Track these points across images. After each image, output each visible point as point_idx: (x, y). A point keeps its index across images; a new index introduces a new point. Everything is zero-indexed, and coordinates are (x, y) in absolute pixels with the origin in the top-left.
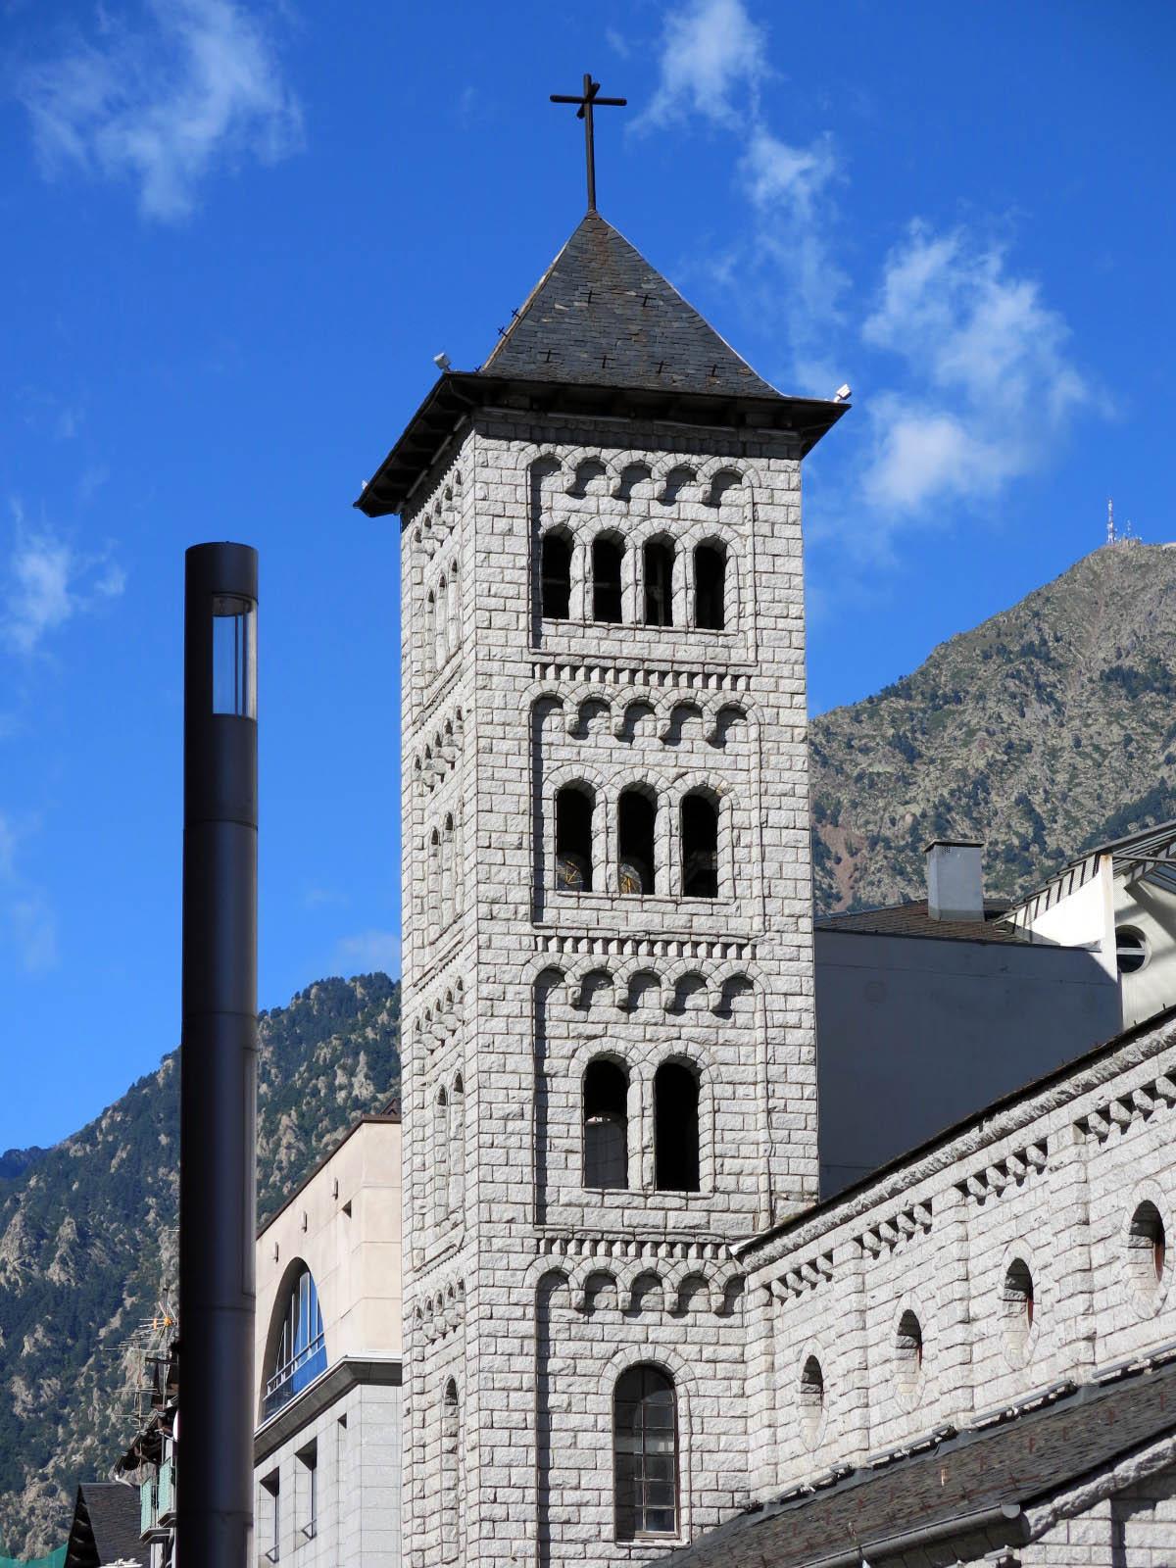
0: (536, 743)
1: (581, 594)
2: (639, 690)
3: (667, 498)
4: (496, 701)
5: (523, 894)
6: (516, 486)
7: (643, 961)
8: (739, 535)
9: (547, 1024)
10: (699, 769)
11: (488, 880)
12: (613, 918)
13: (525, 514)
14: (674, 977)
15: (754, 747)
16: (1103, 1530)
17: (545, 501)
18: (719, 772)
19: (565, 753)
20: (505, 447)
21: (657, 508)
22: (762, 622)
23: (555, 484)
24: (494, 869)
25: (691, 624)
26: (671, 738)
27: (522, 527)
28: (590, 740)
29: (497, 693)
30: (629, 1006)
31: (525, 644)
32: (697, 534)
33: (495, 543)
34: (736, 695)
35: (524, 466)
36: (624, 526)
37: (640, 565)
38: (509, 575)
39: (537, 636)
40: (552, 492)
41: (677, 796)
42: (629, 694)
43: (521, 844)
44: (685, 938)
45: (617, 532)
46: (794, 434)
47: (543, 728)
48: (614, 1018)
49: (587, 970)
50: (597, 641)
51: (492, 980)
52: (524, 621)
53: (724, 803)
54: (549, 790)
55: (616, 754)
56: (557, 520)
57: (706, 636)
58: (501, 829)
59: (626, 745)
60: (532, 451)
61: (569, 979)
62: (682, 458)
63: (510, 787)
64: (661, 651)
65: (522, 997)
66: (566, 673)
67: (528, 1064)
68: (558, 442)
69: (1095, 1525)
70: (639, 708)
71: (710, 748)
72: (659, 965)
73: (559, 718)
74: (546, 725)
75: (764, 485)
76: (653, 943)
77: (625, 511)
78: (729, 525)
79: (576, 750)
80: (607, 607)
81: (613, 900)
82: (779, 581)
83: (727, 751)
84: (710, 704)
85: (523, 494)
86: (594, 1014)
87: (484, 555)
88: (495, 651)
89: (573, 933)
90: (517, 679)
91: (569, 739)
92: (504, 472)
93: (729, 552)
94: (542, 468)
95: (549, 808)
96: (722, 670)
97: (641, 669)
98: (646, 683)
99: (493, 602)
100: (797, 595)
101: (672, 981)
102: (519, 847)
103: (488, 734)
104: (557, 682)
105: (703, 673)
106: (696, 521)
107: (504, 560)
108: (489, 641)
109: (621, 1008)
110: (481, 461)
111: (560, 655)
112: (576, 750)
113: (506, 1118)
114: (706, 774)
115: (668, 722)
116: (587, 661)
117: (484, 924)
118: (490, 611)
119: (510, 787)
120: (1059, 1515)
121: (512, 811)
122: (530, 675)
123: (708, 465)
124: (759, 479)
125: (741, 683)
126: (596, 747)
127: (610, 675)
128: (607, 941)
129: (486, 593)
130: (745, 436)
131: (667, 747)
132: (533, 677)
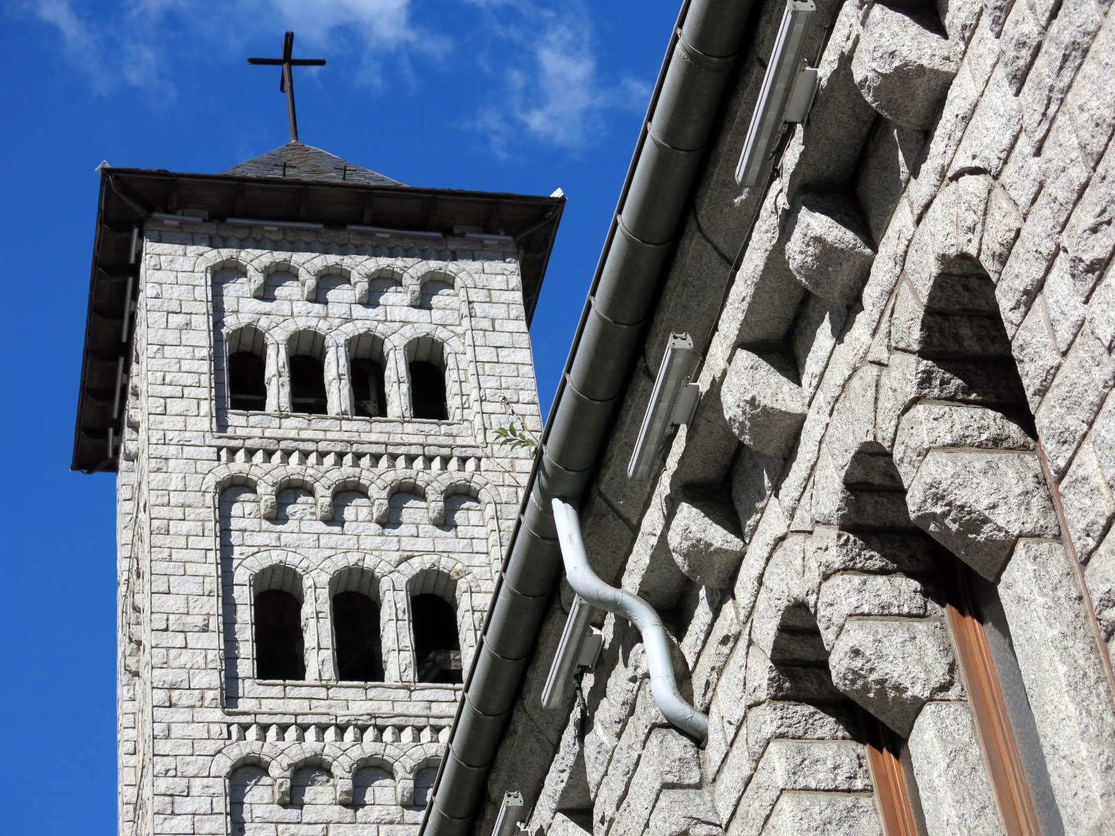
0: (224, 532)
1: (276, 387)
2: (347, 470)
3: (370, 300)
4: (174, 482)
5: (212, 679)
6: (194, 286)
7: (369, 746)
8: (456, 335)
9: (247, 826)
10: (428, 552)
11: (165, 665)
12: (330, 707)
13: (204, 310)
14: (410, 764)
15: (493, 524)
17: (228, 303)
18: (451, 555)
19: (260, 539)
20: (181, 252)
21: (359, 311)
22: (488, 407)
23: (239, 294)
24: (173, 653)
25: (407, 414)
26: (389, 520)
27: (202, 322)
28: (291, 525)
29: (174, 476)
30: (354, 801)
31: (206, 426)
32: (409, 333)
33: (171, 337)
35: (203, 268)
36: (323, 327)
37: (343, 361)
38: (186, 365)
39: (222, 426)
40: (238, 298)
41: (402, 580)
42: (336, 476)
43: (207, 625)
44: (422, 722)
45: (315, 333)
46: (509, 238)
47: (233, 513)
48: (336, 818)
49: (296, 759)
50: (297, 426)
51: (172, 773)
52: (205, 407)
53: (462, 585)
54: (241, 576)
55: (324, 539)
56: (244, 319)
57: (428, 426)
58: (181, 610)
59: (337, 529)
60: (215, 256)
61: (274, 770)
62: (384, 262)
63: (191, 569)
65: (212, 791)
66: (259, 456)
68: (242, 245)
70: (348, 492)
71: (439, 532)
72: (391, 752)
73: (254, 504)
74: (236, 509)
75: (480, 285)
76: (381, 730)
77: (323, 313)
78: (444, 326)
79: (274, 536)
81: (328, 688)
82: (506, 370)
83: (460, 535)
84: (435, 484)
85: (203, 292)
86: (309, 813)
87: (156, 347)
88: (170, 435)
89: (278, 719)
90: (199, 462)
91: (266, 524)
92: (180, 275)
93: (447, 349)
94: (223, 274)
95: (243, 595)
96: (446, 451)
98: (356, 464)
99: (167, 390)
100: (531, 383)
101: (408, 769)
102: (205, 629)
103: (162, 515)
104: (247, 465)
105: (424, 455)
106: (405, 323)
107: (181, 352)
108: (165, 426)
109: (345, 804)
110: (152, 263)
111: (249, 438)
112: (274, 536)
114: (436, 557)
115: (386, 502)
116: (283, 445)
117: (160, 712)
118: (165, 398)
119: (191, 569)
121: (195, 592)
122: (215, 457)
123: (414, 269)
124: (474, 280)
125: (471, 465)
126: (300, 532)
127: (312, 459)
128: (322, 729)
129: (159, 380)
130: (452, 245)
131: (387, 531)
132: (219, 459)
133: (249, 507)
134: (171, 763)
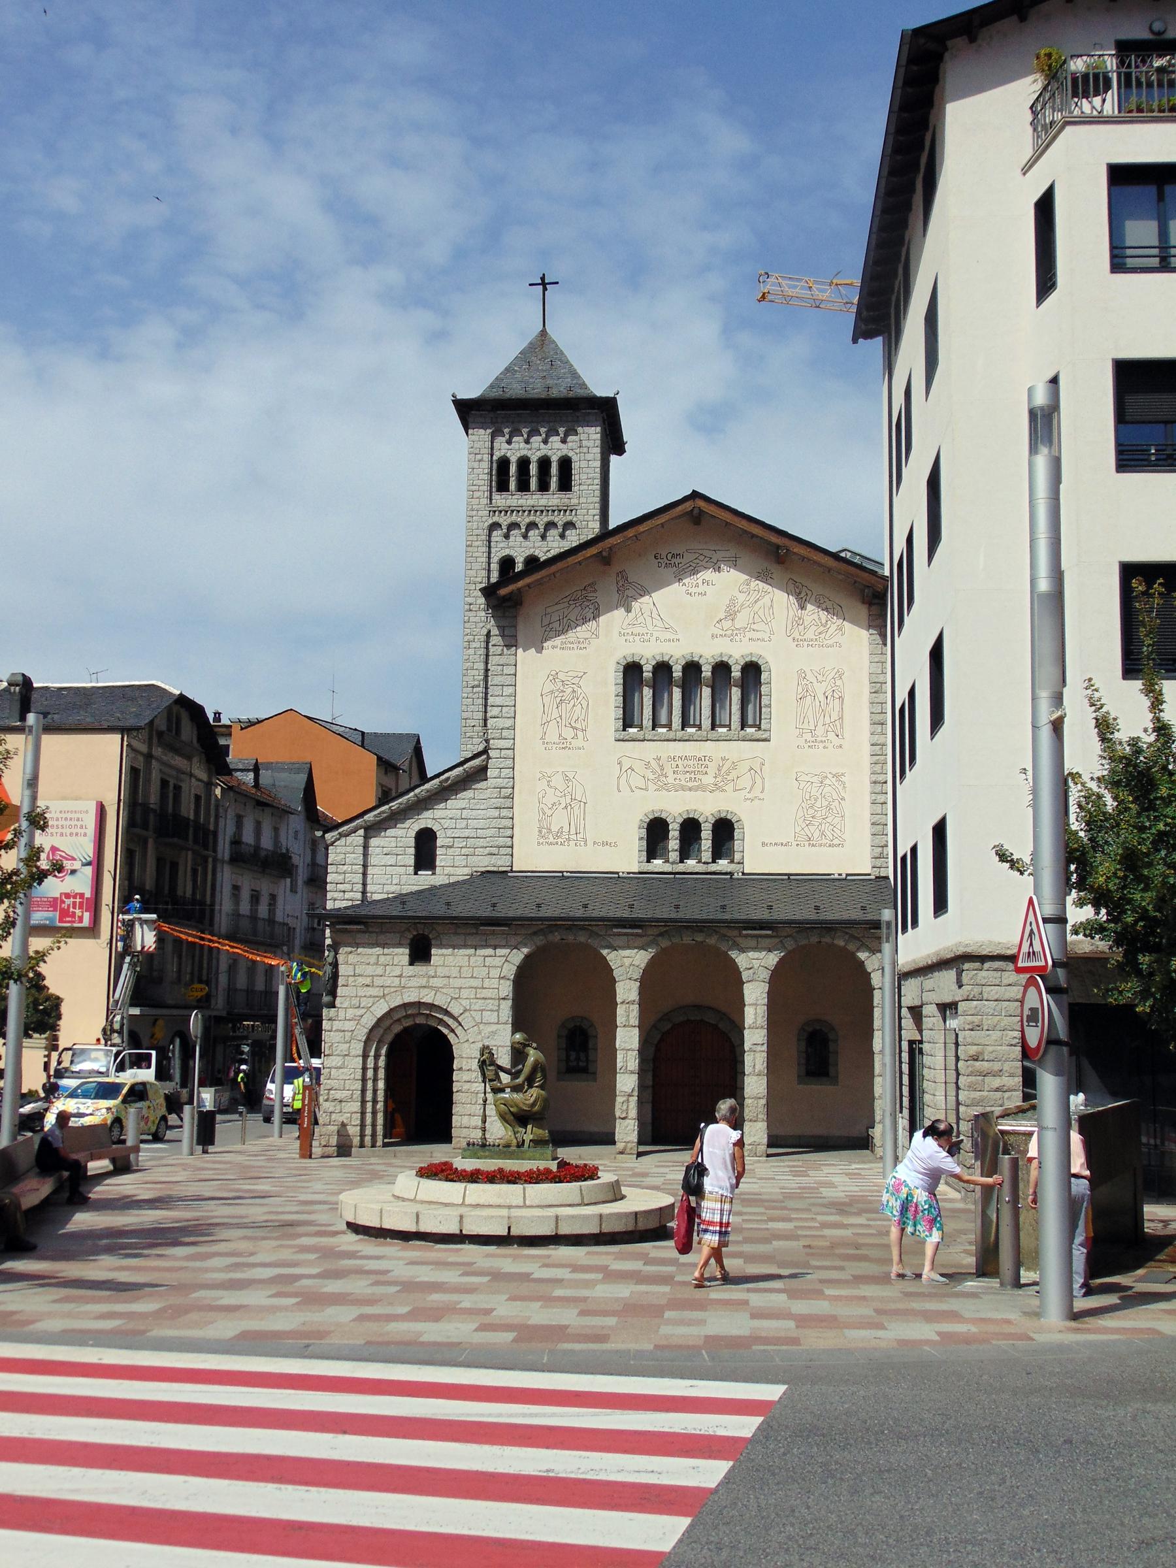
2: (532, 518)
16: (361, 840)
19: (502, 545)
26: (543, 537)
27: (486, 457)
32: (560, 454)
34: (570, 518)
36: (529, 454)
38: (481, 477)
39: (491, 500)
42: (527, 520)
52: (487, 494)
57: (562, 495)
63: (479, 560)
64: (543, 502)
67: (482, 666)
69: (357, 838)
80: (523, 486)
85: (488, 444)
95: (495, 567)
97: (532, 510)
113: (473, 687)
119: (479, 560)
120: (341, 835)
125: (574, 512)
133: (500, 532)
134: (469, 631)
